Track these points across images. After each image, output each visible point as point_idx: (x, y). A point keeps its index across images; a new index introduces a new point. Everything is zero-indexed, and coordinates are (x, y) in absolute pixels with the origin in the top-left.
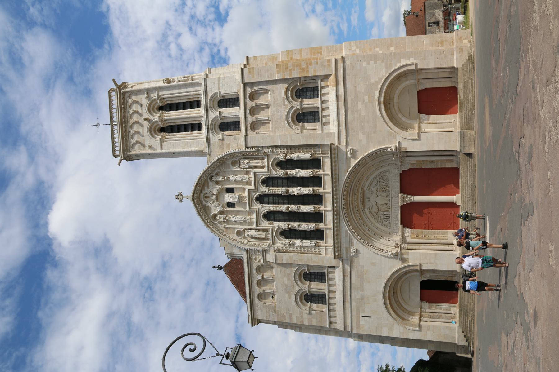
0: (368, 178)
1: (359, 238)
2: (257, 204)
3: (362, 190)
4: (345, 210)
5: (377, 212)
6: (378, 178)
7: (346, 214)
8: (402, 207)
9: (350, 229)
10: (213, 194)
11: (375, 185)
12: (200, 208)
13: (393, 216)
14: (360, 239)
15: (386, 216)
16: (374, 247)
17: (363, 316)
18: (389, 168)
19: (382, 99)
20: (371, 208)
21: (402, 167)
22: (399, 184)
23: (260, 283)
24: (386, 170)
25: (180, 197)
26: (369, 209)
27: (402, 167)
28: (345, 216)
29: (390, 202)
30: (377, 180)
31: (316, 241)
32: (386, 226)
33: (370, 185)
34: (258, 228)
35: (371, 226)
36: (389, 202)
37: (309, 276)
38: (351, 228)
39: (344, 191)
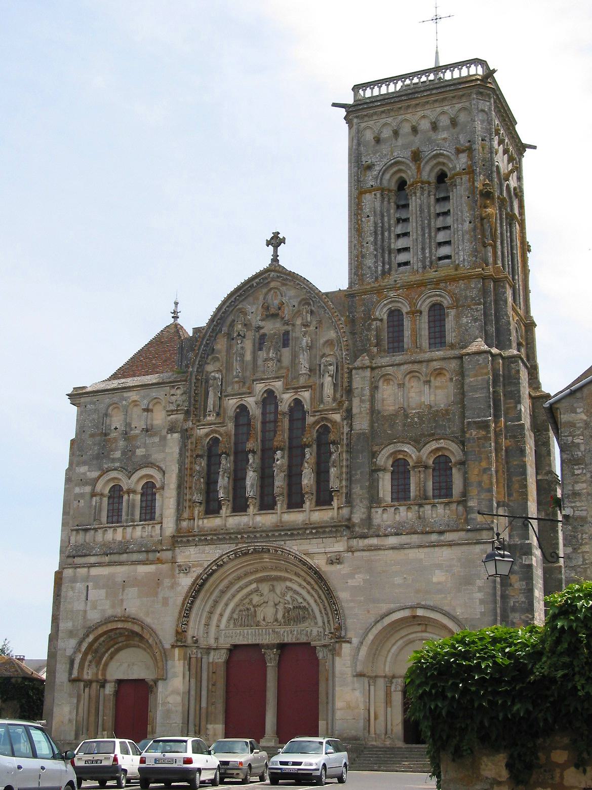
0: (303, 588)
2: (261, 393)
6: (305, 604)
8: (256, 647)
10: (280, 309)
11: (294, 600)
12: (255, 284)
14: (202, 579)
17: (88, 586)
18: (320, 623)
19: (420, 612)
22: (294, 641)
23: (136, 405)
25: (276, 241)
31: (204, 502)
32: (230, 618)
34: (223, 397)
35: (228, 595)
37: (149, 492)
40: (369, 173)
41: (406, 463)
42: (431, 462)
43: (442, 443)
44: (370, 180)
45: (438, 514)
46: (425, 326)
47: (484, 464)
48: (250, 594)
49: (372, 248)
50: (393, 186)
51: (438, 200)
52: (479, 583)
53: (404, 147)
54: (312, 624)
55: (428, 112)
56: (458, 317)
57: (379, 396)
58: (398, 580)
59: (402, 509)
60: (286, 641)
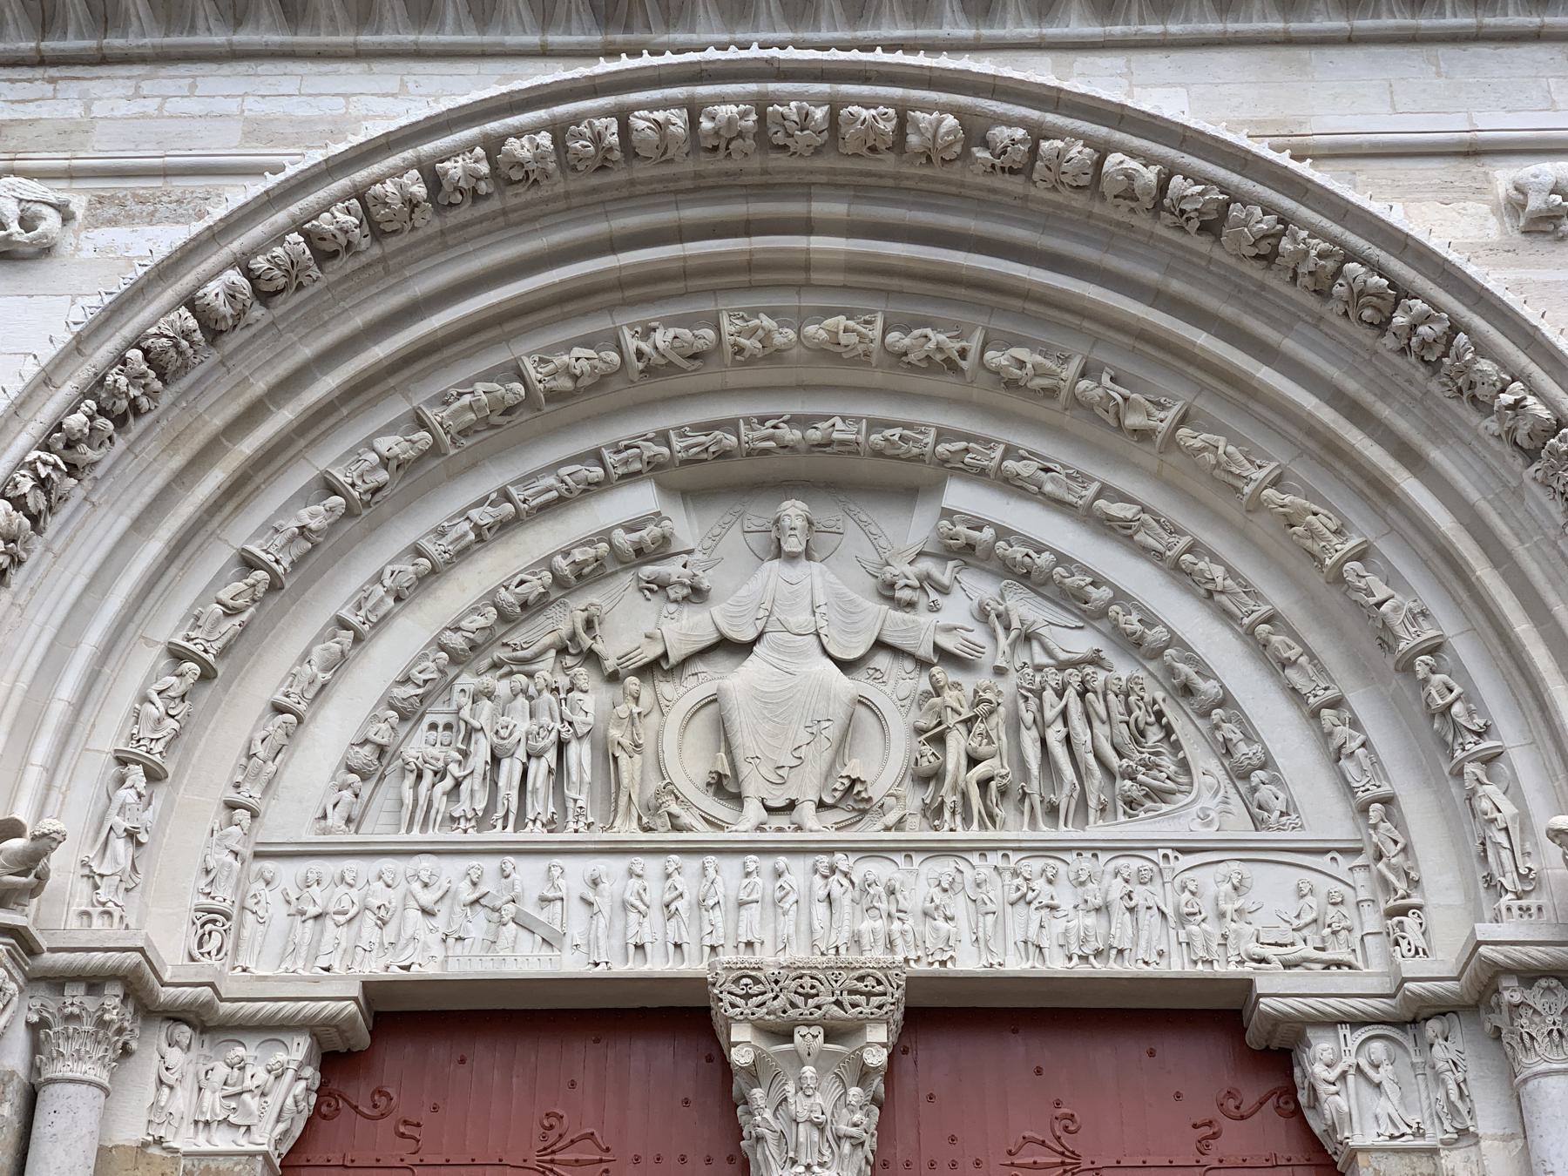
1: (214, 288)
3: (943, 435)
4: (677, 119)
5: (591, 657)
7: (615, 139)
9: (376, 169)
13: (538, 865)
15: (538, 770)
16: (26, 485)
20: (671, 569)
21: (1356, 1022)
22: (1057, 965)
24: (1276, 780)
26: (649, 533)
27: (1356, 1022)
28: (576, 119)
29: (760, 828)
30: (1096, 660)
33: (1018, 552)
36: (753, 812)
38: (389, 187)
39: (957, 112)
48: (585, 577)
54: (1239, 827)
60: (968, 962)
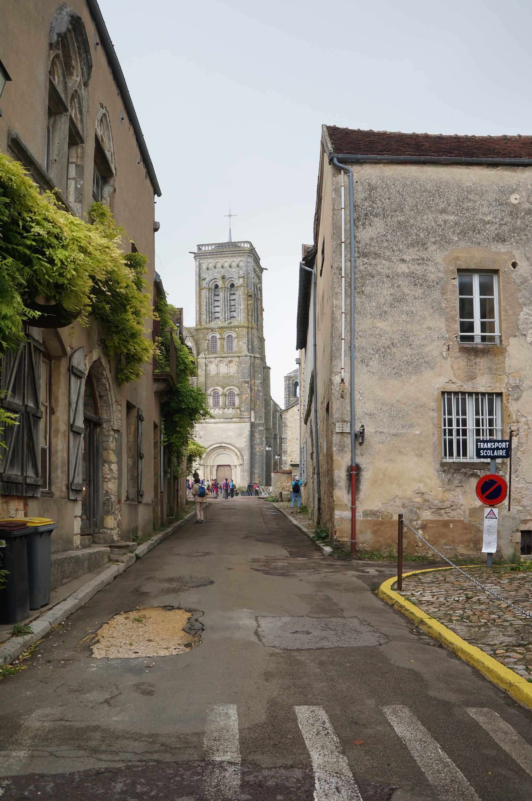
19: (223, 445)
40: (204, 282)
41: (218, 393)
42: (227, 393)
43: (232, 387)
44: (204, 284)
45: (230, 411)
46: (225, 344)
47: (247, 396)
49: (205, 311)
50: (213, 287)
51: (231, 294)
52: (244, 436)
53: (218, 273)
55: (228, 260)
56: (238, 342)
57: (208, 368)
58: (215, 434)
59: (217, 409)
